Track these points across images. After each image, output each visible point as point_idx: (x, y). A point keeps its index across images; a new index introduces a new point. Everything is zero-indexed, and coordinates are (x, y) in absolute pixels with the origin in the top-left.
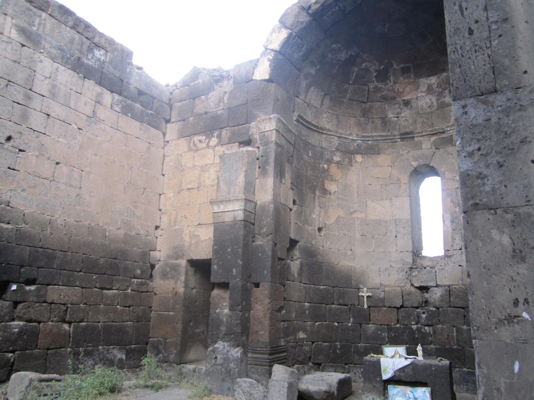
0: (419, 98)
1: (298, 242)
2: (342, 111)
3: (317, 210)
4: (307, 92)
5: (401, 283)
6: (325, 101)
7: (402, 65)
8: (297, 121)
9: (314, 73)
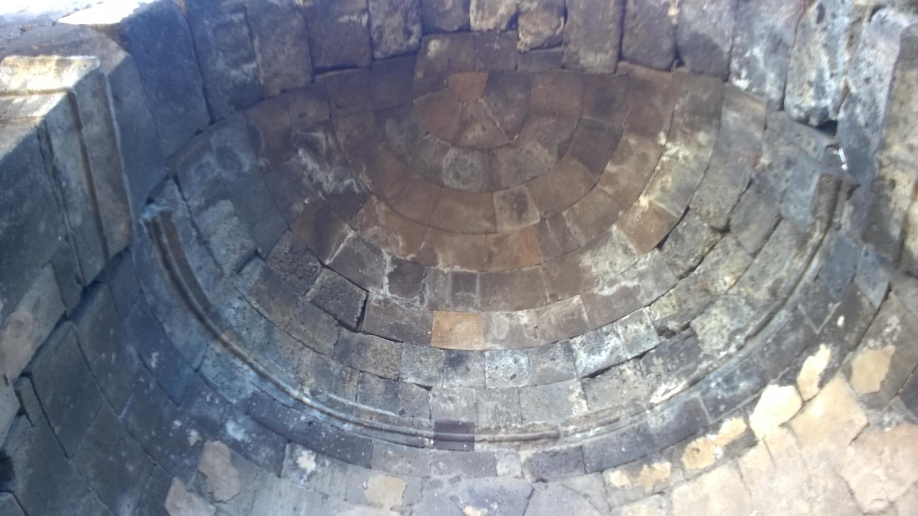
0: (487, 354)
2: (287, 319)
4: (210, 202)
6: (247, 269)
7: (457, 268)
9: (246, 168)
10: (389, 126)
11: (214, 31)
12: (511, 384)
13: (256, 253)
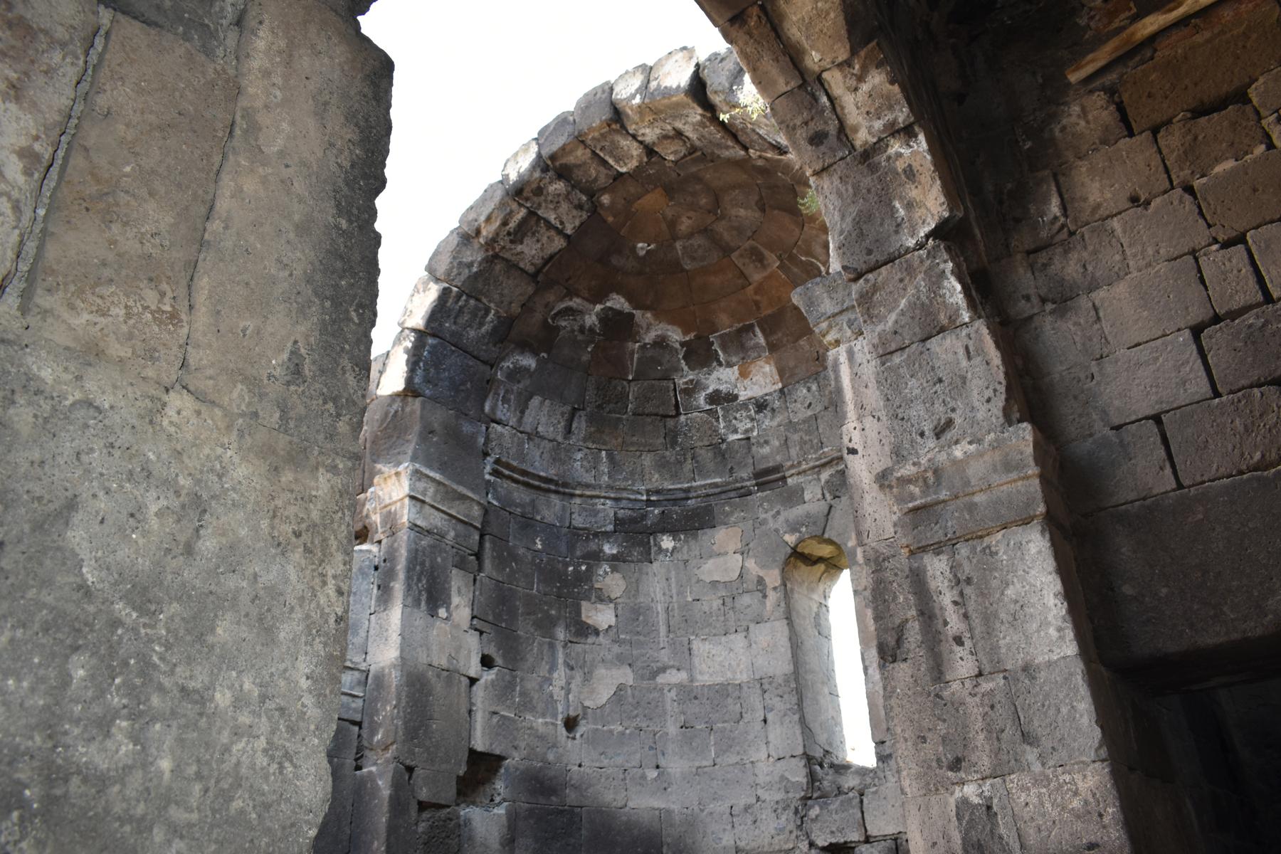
1: (504, 758)
2: (620, 440)
3: (560, 676)
5: (787, 841)
6: (574, 426)
8: (495, 473)
10: (615, 260)
11: (455, 323)
12: (810, 413)
13: (574, 409)
